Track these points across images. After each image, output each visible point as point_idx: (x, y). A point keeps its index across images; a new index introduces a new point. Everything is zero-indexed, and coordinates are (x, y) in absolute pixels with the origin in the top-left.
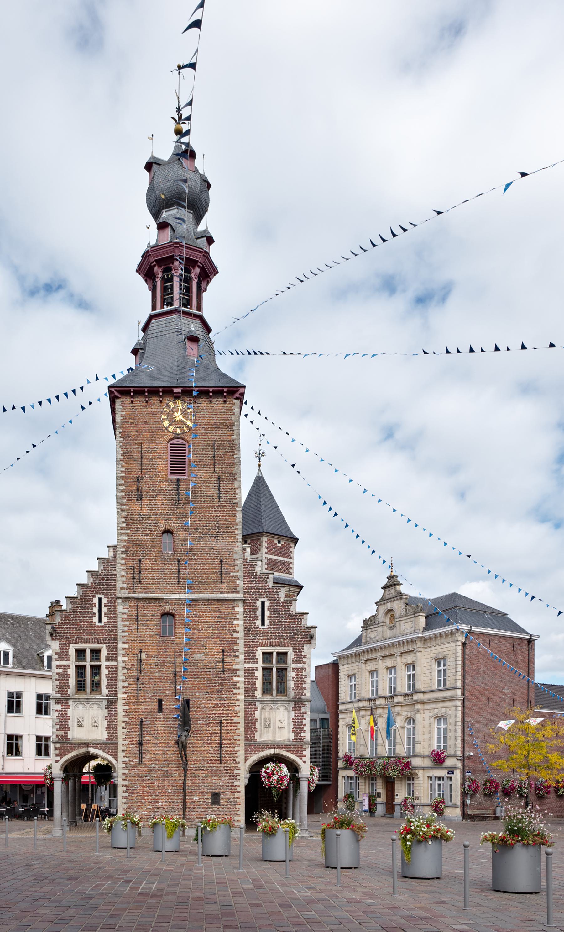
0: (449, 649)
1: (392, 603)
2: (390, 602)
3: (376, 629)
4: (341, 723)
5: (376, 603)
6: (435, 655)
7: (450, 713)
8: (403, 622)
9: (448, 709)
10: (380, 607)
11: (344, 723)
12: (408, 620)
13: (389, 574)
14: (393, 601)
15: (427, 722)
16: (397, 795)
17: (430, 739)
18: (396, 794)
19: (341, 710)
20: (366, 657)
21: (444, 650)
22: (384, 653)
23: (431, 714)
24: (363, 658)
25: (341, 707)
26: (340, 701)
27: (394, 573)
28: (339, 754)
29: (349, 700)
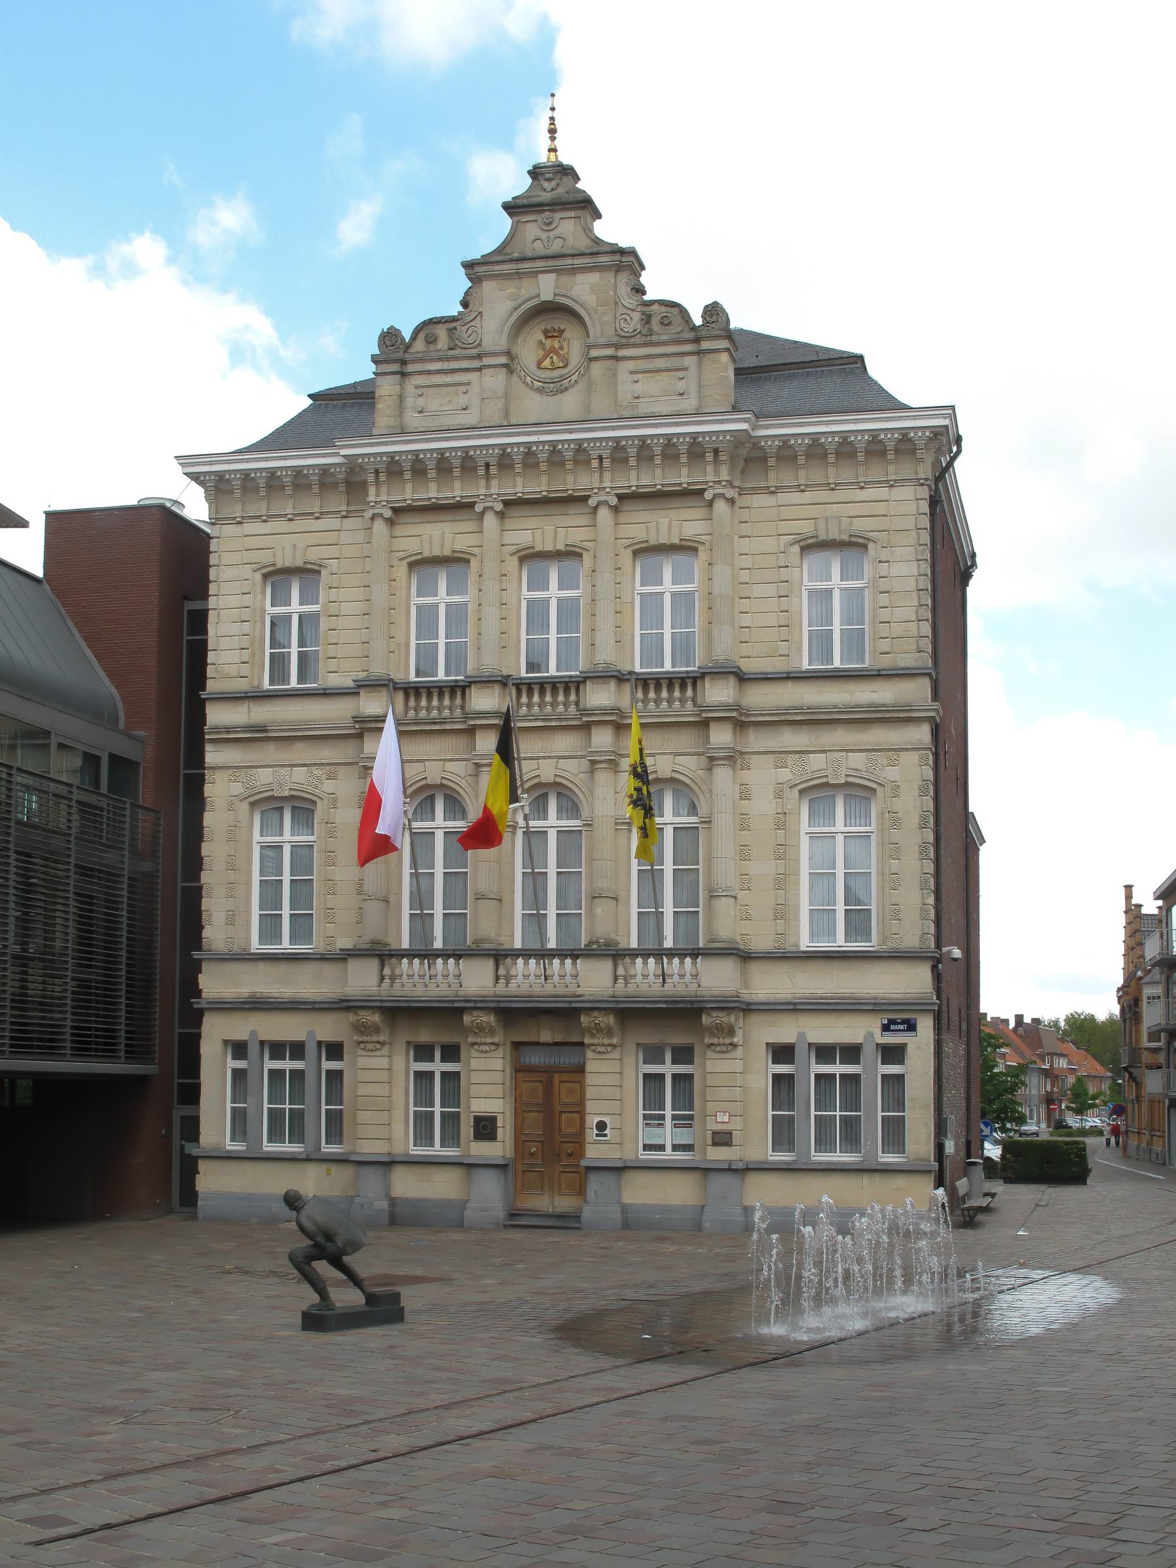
1: (565, 279)
2: (559, 271)
4: (217, 789)
5: (469, 266)
8: (631, 365)
9: (881, 758)
10: (488, 286)
11: (237, 788)
12: (661, 363)
13: (543, 157)
14: (574, 271)
15: (763, 806)
18: (592, 1121)
19: (217, 729)
20: (408, 493)
22: (521, 486)
23: (785, 775)
24: (381, 497)
25: (217, 716)
26: (212, 686)
27: (565, 158)
28: (206, 933)
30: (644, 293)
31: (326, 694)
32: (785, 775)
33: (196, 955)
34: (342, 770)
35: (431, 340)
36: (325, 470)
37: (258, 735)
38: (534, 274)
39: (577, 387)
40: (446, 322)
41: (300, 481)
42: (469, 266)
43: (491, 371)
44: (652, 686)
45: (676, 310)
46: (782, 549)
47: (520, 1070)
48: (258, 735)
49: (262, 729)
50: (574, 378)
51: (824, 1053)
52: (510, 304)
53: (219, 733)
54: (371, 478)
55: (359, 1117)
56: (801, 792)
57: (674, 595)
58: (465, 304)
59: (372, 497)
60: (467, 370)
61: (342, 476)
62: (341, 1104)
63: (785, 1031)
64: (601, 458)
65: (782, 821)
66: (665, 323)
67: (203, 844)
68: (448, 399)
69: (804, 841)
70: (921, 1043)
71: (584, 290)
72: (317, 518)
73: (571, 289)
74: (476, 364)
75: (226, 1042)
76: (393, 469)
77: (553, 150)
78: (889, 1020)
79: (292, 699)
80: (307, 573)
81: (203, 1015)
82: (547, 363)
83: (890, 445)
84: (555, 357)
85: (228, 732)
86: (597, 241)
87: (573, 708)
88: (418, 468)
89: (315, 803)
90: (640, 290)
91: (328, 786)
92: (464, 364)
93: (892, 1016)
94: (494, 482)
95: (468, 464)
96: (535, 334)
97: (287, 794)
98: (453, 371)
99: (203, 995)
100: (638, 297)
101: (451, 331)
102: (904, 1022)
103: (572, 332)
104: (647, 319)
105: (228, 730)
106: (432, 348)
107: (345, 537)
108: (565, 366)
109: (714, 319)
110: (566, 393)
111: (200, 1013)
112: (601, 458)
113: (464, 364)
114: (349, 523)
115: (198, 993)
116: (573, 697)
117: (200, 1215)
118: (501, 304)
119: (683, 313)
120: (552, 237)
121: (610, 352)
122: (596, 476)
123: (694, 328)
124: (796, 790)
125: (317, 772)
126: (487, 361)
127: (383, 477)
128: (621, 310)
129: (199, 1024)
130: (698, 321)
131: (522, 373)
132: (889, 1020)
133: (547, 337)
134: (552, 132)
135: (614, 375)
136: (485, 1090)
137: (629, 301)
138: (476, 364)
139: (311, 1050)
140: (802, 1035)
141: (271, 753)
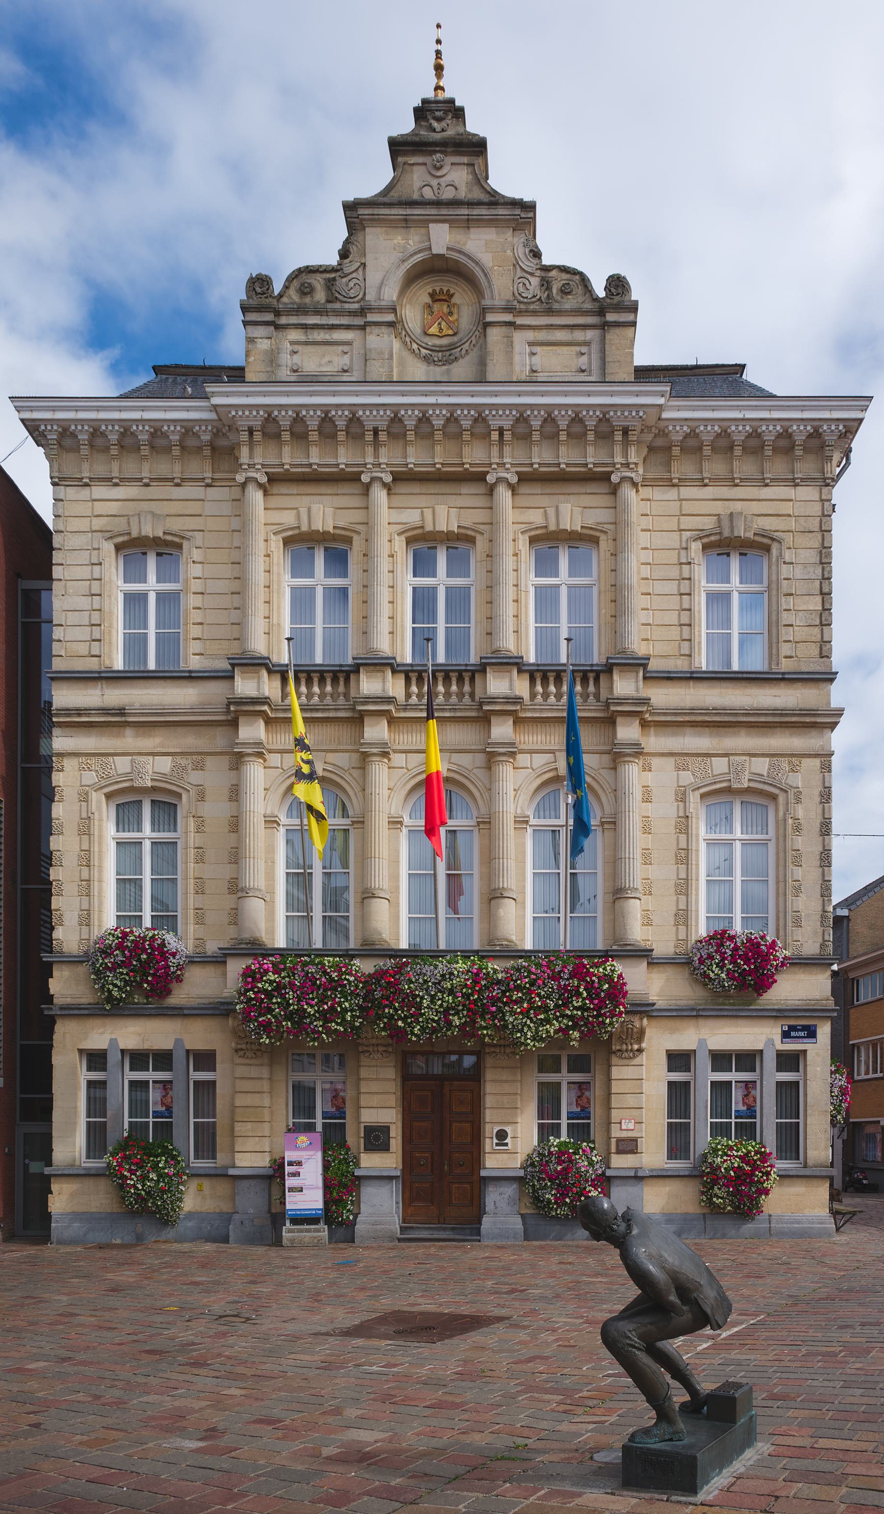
0: (787, 508)
2: (453, 222)
3: (338, 335)
4: (66, 778)
6: (708, 523)
7: (797, 780)
8: (530, 335)
9: (785, 764)
15: (664, 810)
16: (502, 1135)
17: (684, 887)
19: (67, 711)
21: (756, 507)
22: (415, 457)
23: (687, 778)
28: (58, 934)
29: (119, 664)
30: (540, 258)
31: (191, 677)
32: (687, 778)
33: (46, 958)
34: (209, 761)
35: (306, 290)
36: (188, 429)
37: (115, 720)
38: (425, 223)
39: (467, 358)
40: (325, 271)
41: (158, 440)
42: (351, 208)
43: (376, 330)
44: (552, 679)
45: (577, 277)
46: (684, 545)
47: (407, 1079)
48: (115, 720)
49: (121, 711)
50: (466, 346)
51: (721, 1060)
52: (396, 256)
53: (69, 715)
54: (244, 436)
55: (236, 1129)
56: (703, 796)
57: (570, 587)
58: (344, 254)
59: (244, 458)
60: (348, 327)
61: (206, 437)
62: (214, 1117)
63: (687, 1037)
64: (501, 431)
65: (684, 824)
66: (565, 291)
67: (52, 838)
68: (327, 359)
69: (703, 846)
70: (818, 1051)
71: (482, 246)
72: (178, 485)
73: (464, 244)
74: (359, 321)
75: (81, 1051)
76: (270, 428)
77: (438, 88)
78: (789, 1026)
79: (154, 682)
80: (167, 548)
81: (54, 1022)
82: (434, 330)
83: (799, 438)
84: (443, 323)
85: (79, 715)
86: (494, 193)
87: (467, 699)
88: (299, 431)
89: (179, 796)
90: (536, 254)
91: (195, 777)
92: (344, 321)
93: (793, 1022)
94: (383, 451)
95: (355, 427)
96: (422, 294)
97: (149, 784)
98: (333, 327)
99: (55, 1001)
100: (535, 261)
101: (330, 284)
102: (804, 1028)
103: (462, 297)
104: (546, 284)
105: (79, 711)
106: (308, 300)
107: (209, 508)
108: (455, 334)
109: (620, 290)
110: (455, 364)
111: (51, 1022)
112: (501, 431)
113: (344, 321)
114: (213, 493)
115: (50, 999)
116: (467, 688)
117: (54, 1235)
118: (388, 255)
119: (584, 280)
120: (444, 185)
121: (508, 317)
122: (495, 451)
123: (596, 299)
124: (697, 794)
125: (182, 761)
126: (371, 318)
127: (257, 436)
128: (519, 273)
129: (51, 1032)
130: (601, 293)
131: (408, 339)
132: (789, 1026)
133: (435, 301)
134: (439, 69)
135: (511, 344)
136: (375, 1100)
137: (529, 264)
138: (359, 321)
139: (179, 1059)
140: (702, 1042)
141: (130, 740)
